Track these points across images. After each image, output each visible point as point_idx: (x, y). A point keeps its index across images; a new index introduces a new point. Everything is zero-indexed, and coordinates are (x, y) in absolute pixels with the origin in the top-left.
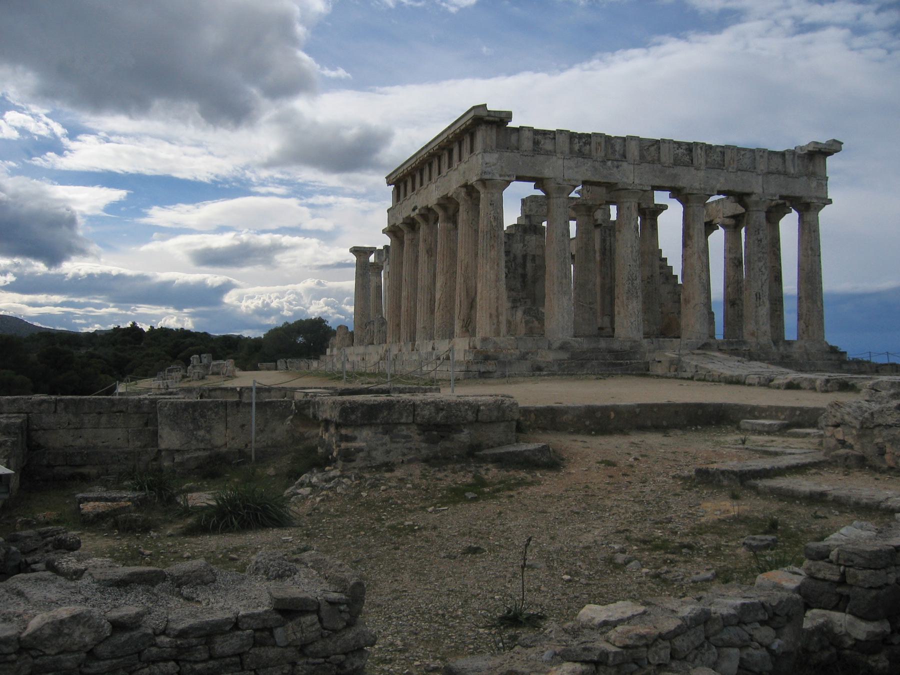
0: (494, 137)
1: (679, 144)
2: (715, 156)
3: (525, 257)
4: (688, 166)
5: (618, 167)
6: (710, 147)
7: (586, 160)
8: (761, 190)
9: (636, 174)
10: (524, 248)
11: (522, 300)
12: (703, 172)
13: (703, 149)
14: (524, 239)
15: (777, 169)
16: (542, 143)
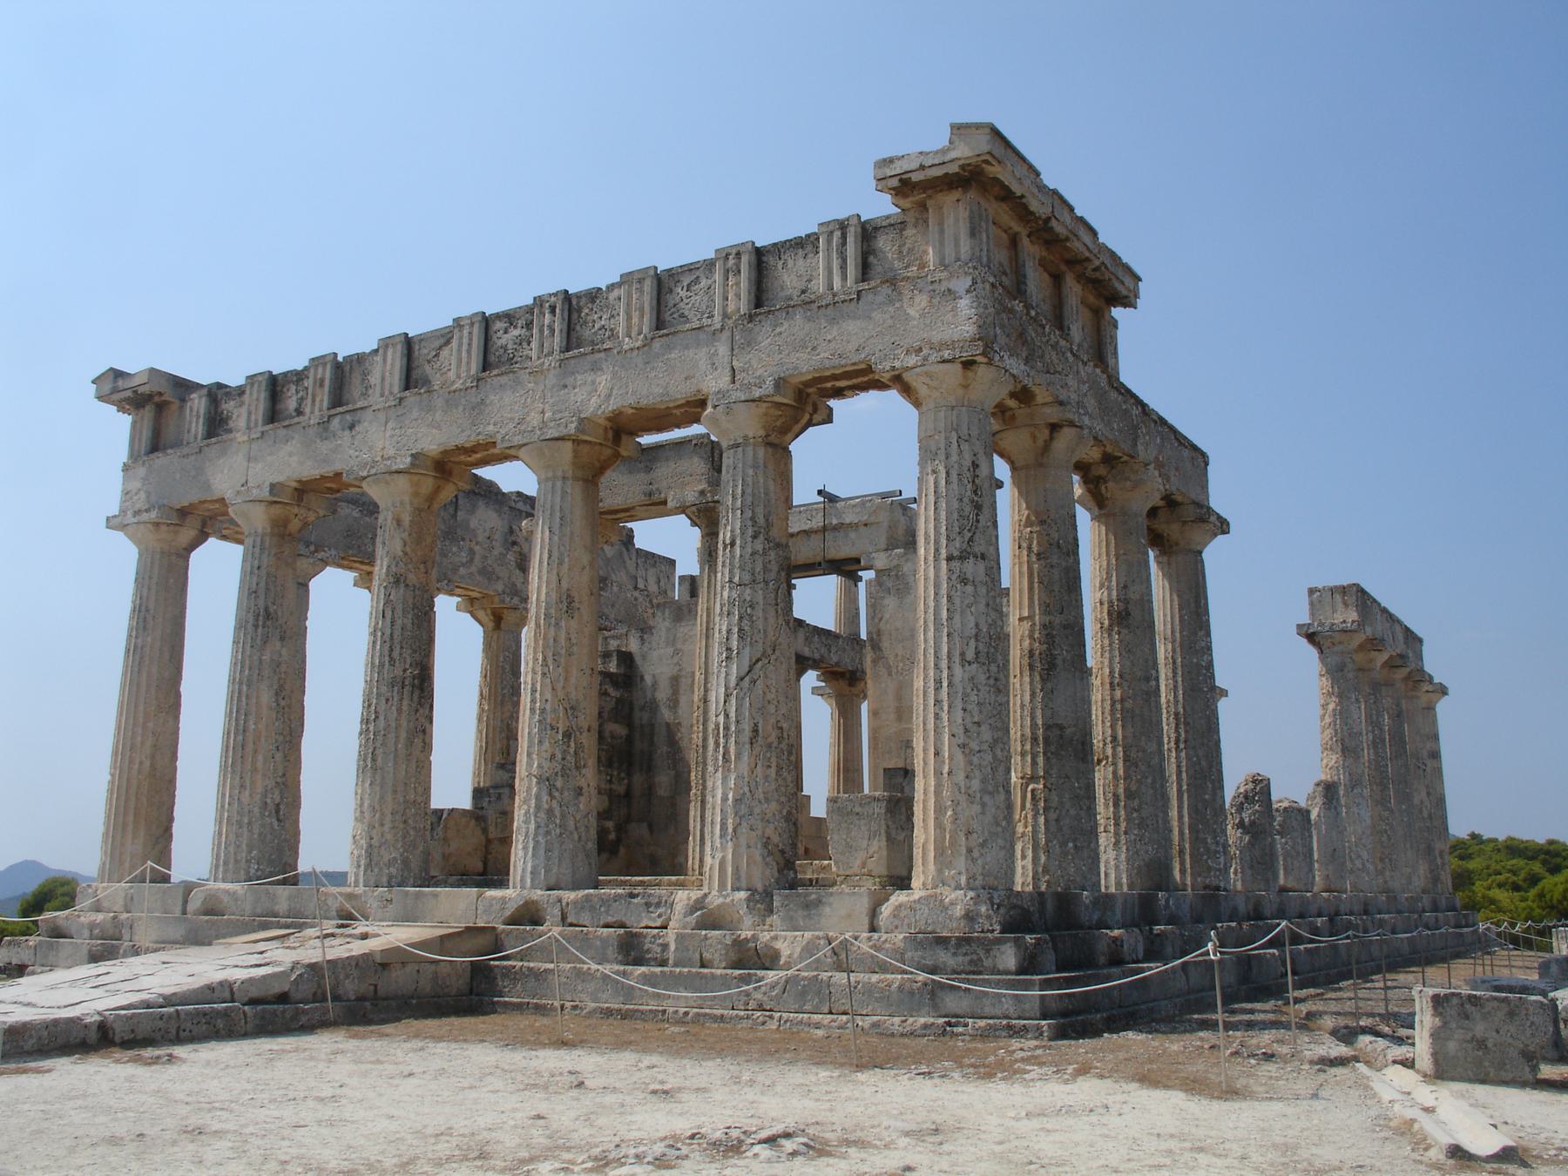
0: (146, 434)
1: (509, 317)
2: (604, 317)
3: (675, 681)
4: (514, 372)
5: (352, 427)
6: (593, 295)
7: (290, 432)
8: (728, 379)
9: (387, 435)
10: (676, 660)
11: (491, 791)
12: (552, 372)
13: (557, 311)
14: (675, 636)
15: (803, 292)
16: (234, 417)
